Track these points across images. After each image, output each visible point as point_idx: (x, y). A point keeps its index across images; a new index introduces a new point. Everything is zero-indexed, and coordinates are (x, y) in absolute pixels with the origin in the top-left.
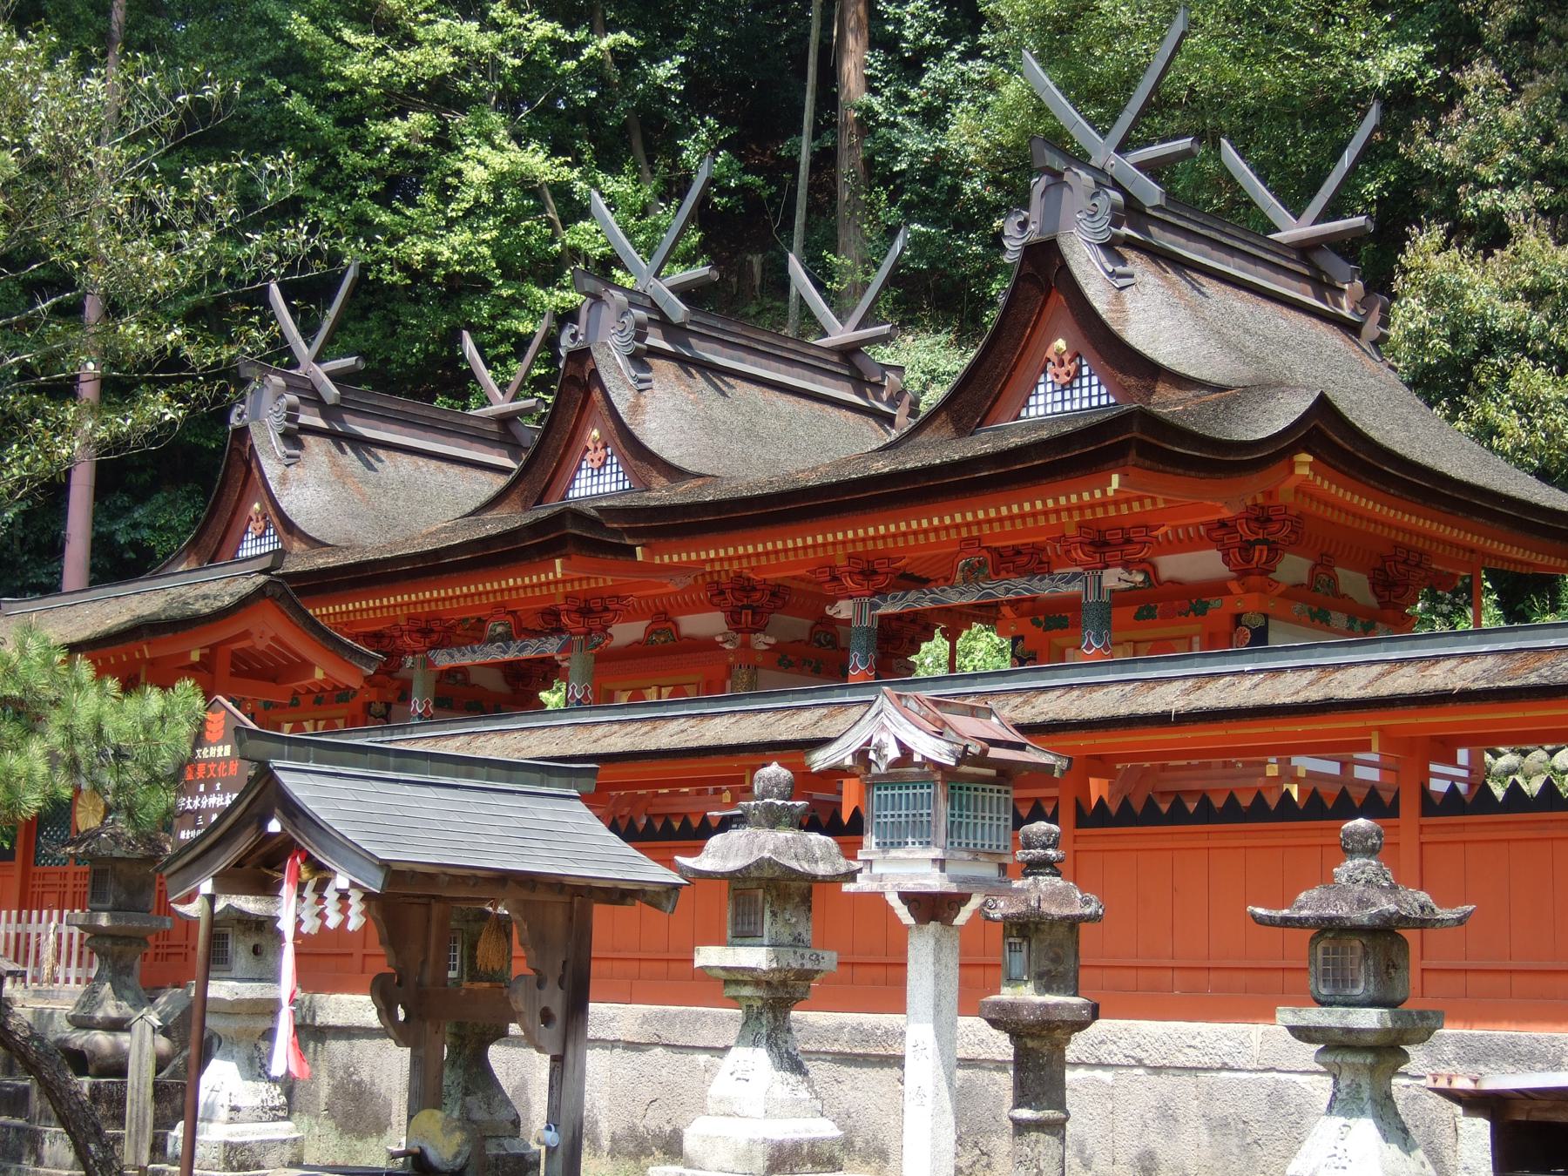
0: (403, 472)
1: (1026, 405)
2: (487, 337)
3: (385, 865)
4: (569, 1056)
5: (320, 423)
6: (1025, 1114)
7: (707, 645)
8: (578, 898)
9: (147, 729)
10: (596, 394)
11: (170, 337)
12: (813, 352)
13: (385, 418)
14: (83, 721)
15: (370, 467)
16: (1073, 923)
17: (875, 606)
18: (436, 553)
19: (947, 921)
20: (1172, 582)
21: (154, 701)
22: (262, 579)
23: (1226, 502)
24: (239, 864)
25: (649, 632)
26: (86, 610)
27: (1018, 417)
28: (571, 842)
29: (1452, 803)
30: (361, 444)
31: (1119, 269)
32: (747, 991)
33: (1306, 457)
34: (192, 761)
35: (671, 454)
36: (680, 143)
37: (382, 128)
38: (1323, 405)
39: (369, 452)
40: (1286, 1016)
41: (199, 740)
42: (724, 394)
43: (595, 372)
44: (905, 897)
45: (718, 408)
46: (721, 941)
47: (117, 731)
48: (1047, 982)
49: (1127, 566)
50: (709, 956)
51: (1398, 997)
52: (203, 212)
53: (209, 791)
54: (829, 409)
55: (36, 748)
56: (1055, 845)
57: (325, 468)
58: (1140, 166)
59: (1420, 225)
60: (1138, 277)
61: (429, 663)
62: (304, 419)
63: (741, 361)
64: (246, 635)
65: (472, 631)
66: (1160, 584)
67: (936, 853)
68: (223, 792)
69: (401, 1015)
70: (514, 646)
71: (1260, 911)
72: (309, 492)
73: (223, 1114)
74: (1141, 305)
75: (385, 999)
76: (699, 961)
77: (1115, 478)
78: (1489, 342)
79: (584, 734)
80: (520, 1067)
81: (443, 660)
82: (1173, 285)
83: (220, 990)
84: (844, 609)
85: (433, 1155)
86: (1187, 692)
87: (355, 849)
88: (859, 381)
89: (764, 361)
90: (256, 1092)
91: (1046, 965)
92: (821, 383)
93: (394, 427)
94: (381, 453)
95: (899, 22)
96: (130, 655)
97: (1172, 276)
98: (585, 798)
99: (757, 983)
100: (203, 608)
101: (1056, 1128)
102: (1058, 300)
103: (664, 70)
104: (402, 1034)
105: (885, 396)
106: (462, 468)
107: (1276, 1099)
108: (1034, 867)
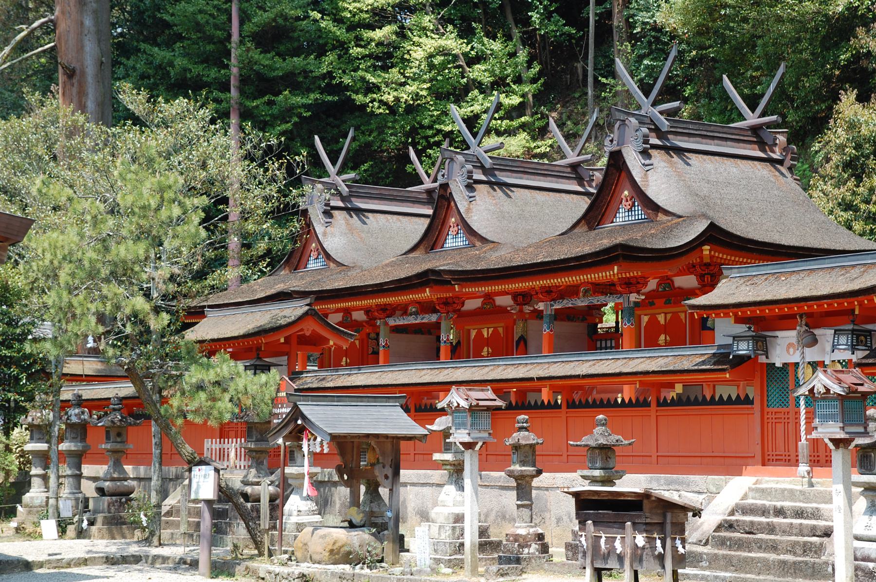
0: (381, 224)
1: (615, 216)
2: (430, 132)
3: (330, 434)
4: (394, 489)
5: (341, 204)
6: (519, 503)
7: (503, 310)
8: (396, 440)
9: (261, 387)
10: (452, 204)
11: (265, 226)
12: (557, 169)
14: (241, 387)
15: (364, 223)
16: (532, 446)
17: (552, 305)
18: (381, 284)
19: (473, 449)
20: (679, 288)
21: (263, 377)
22: (307, 308)
23: (684, 261)
24: (290, 433)
25: (483, 303)
26: (240, 318)
27: (612, 222)
28: (392, 420)
29: (679, 402)
30: (359, 211)
31: (647, 162)
32: (448, 467)
33: (707, 247)
34: (277, 397)
35: (482, 232)
36: (530, 14)
37: (368, 34)
38: (712, 226)
39: (364, 216)
40: (580, 472)
41: (278, 391)
42: (510, 197)
43: (451, 193)
44: (461, 443)
46: (440, 451)
47: (252, 390)
48: (523, 463)
49: (638, 293)
50: (437, 456)
51: (611, 466)
52: (273, 180)
53: (282, 407)
54: (563, 195)
55: (227, 396)
56: (526, 422)
57: (344, 227)
58: (661, 113)
59: (846, 91)
60: (655, 165)
61: (387, 324)
62: (333, 203)
63: (521, 178)
64: (302, 330)
65: (404, 310)
66: (675, 289)
67: (467, 431)
68: (287, 407)
69: (346, 477)
70: (420, 317)
71: (571, 443)
72: (336, 240)
73: (295, 513)
74: (655, 178)
75: (340, 471)
76: (434, 458)
77: (616, 267)
79: (418, 373)
80: (384, 492)
81: (392, 322)
82: (672, 165)
83: (288, 470)
84: (541, 306)
85: (354, 521)
86: (590, 366)
87: (321, 430)
88: (580, 180)
89: (532, 177)
90: (307, 505)
91: (523, 458)
92: (561, 183)
93: (376, 201)
94: (370, 215)
96: (258, 341)
97: (676, 159)
98: (402, 407)
99: (451, 465)
100: (283, 322)
101: (530, 507)
102: (623, 174)
104: (347, 484)
105: (594, 184)
106: (410, 218)
108: (521, 429)
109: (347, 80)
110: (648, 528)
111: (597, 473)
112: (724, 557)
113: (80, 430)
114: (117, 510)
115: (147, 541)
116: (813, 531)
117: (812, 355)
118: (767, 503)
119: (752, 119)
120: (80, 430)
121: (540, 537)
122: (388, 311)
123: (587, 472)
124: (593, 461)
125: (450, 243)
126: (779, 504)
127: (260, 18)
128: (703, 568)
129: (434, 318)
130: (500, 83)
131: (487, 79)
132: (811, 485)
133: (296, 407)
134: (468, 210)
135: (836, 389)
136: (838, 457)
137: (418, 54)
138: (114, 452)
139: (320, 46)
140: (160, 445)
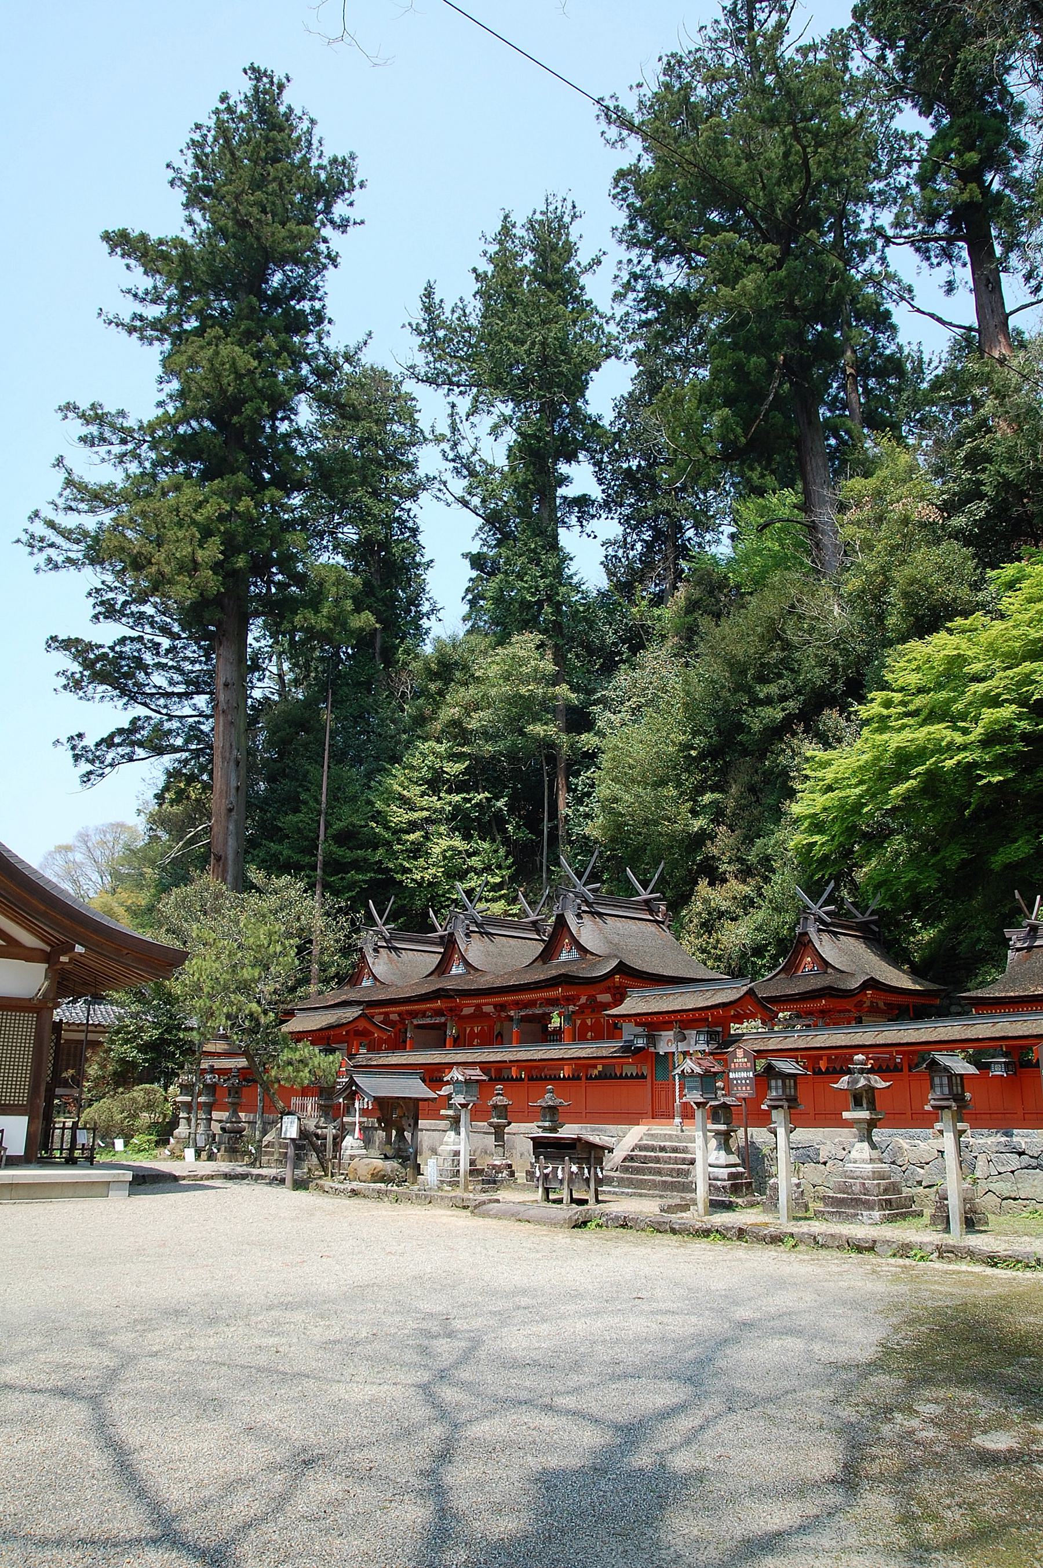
7: (487, 1015)
13: (404, 940)
28: (415, 1088)
29: (600, 1077)
37: (407, 837)
45: (491, 947)
50: (443, 1112)
52: (342, 928)
55: (307, 1070)
65: (423, 1014)
75: (379, 1121)
78: (721, 914)
80: (407, 1135)
82: (596, 923)
83: (345, 1119)
84: (512, 1013)
95: (577, 785)
101: (503, 1146)
103: (500, 804)
109: (391, 866)
110: (579, 1161)
111: (547, 1124)
113: (211, 1089)
114: (233, 1142)
115: (252, 1164)
116: (684, 1161)
117: (682, 1047)
119: (645, 895)
120: (211, 1089)
121: (510, 1166)
122: (414, 1014)
123: (540, 1124)
124: (544, 1116)
125: (454, 971)
127: (339, 825)
129: (443, 1020)
130: (488, 869)
131: (480, 866)
133: (351, 1078)
134: (466, 950)
135: (698, 1070)
136: (699, 1114)
137: (437, 850)
138: (233, 1104)
139: (374, 843)
140: (263, 1100)
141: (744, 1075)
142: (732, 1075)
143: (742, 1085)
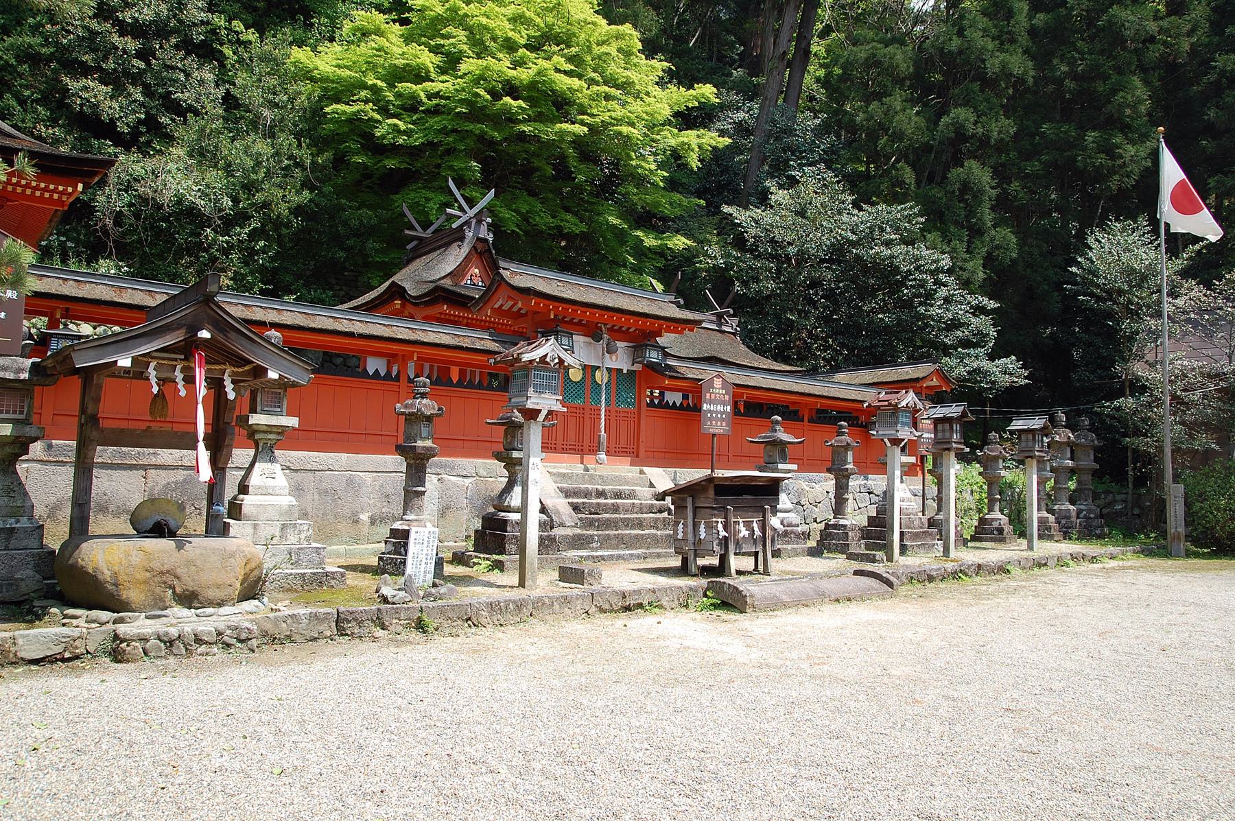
107: (350, 482)
112: (616, 536)
118: (590, 487)
126: (600, 488)
128: (593, 549)
132: (587, 470)
141: (720, 408)
142: (705, 407)
143: (716, 419)
